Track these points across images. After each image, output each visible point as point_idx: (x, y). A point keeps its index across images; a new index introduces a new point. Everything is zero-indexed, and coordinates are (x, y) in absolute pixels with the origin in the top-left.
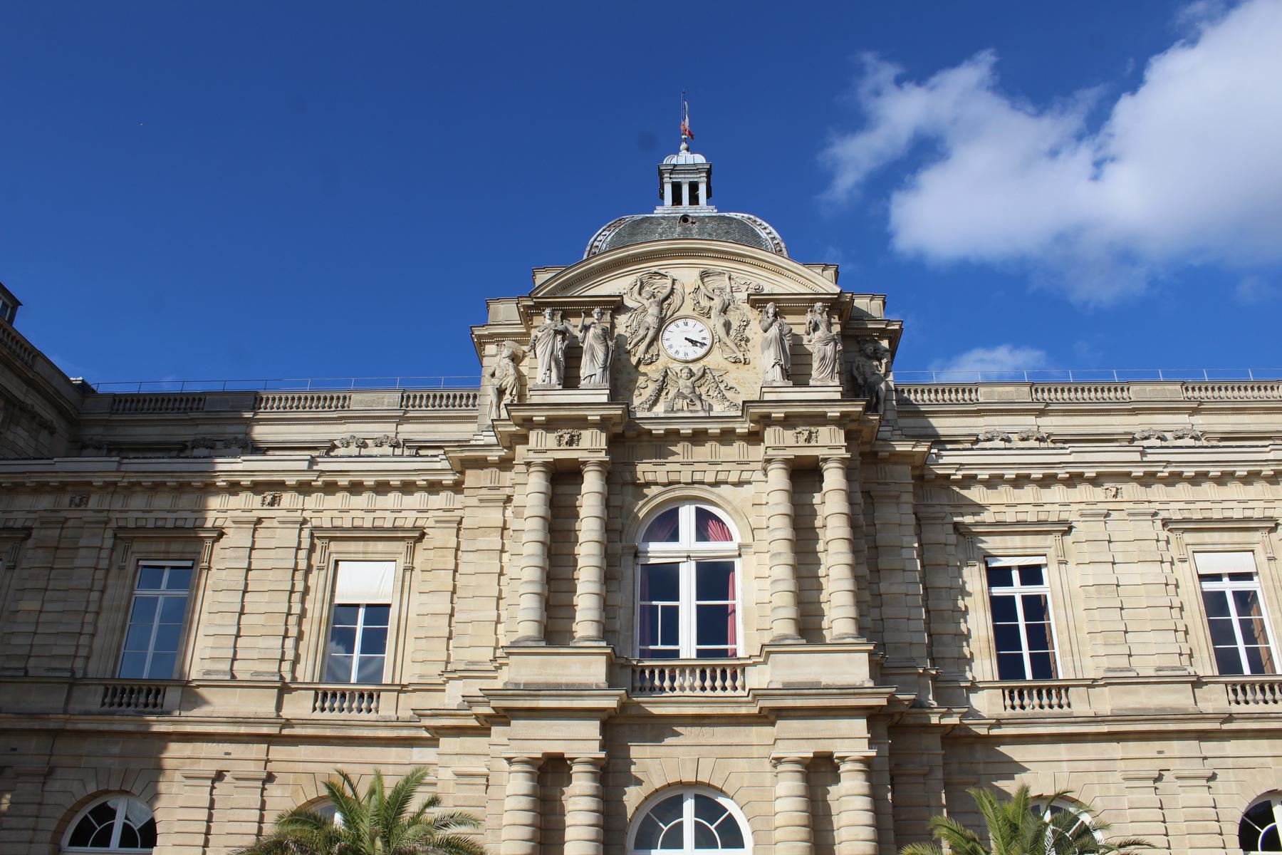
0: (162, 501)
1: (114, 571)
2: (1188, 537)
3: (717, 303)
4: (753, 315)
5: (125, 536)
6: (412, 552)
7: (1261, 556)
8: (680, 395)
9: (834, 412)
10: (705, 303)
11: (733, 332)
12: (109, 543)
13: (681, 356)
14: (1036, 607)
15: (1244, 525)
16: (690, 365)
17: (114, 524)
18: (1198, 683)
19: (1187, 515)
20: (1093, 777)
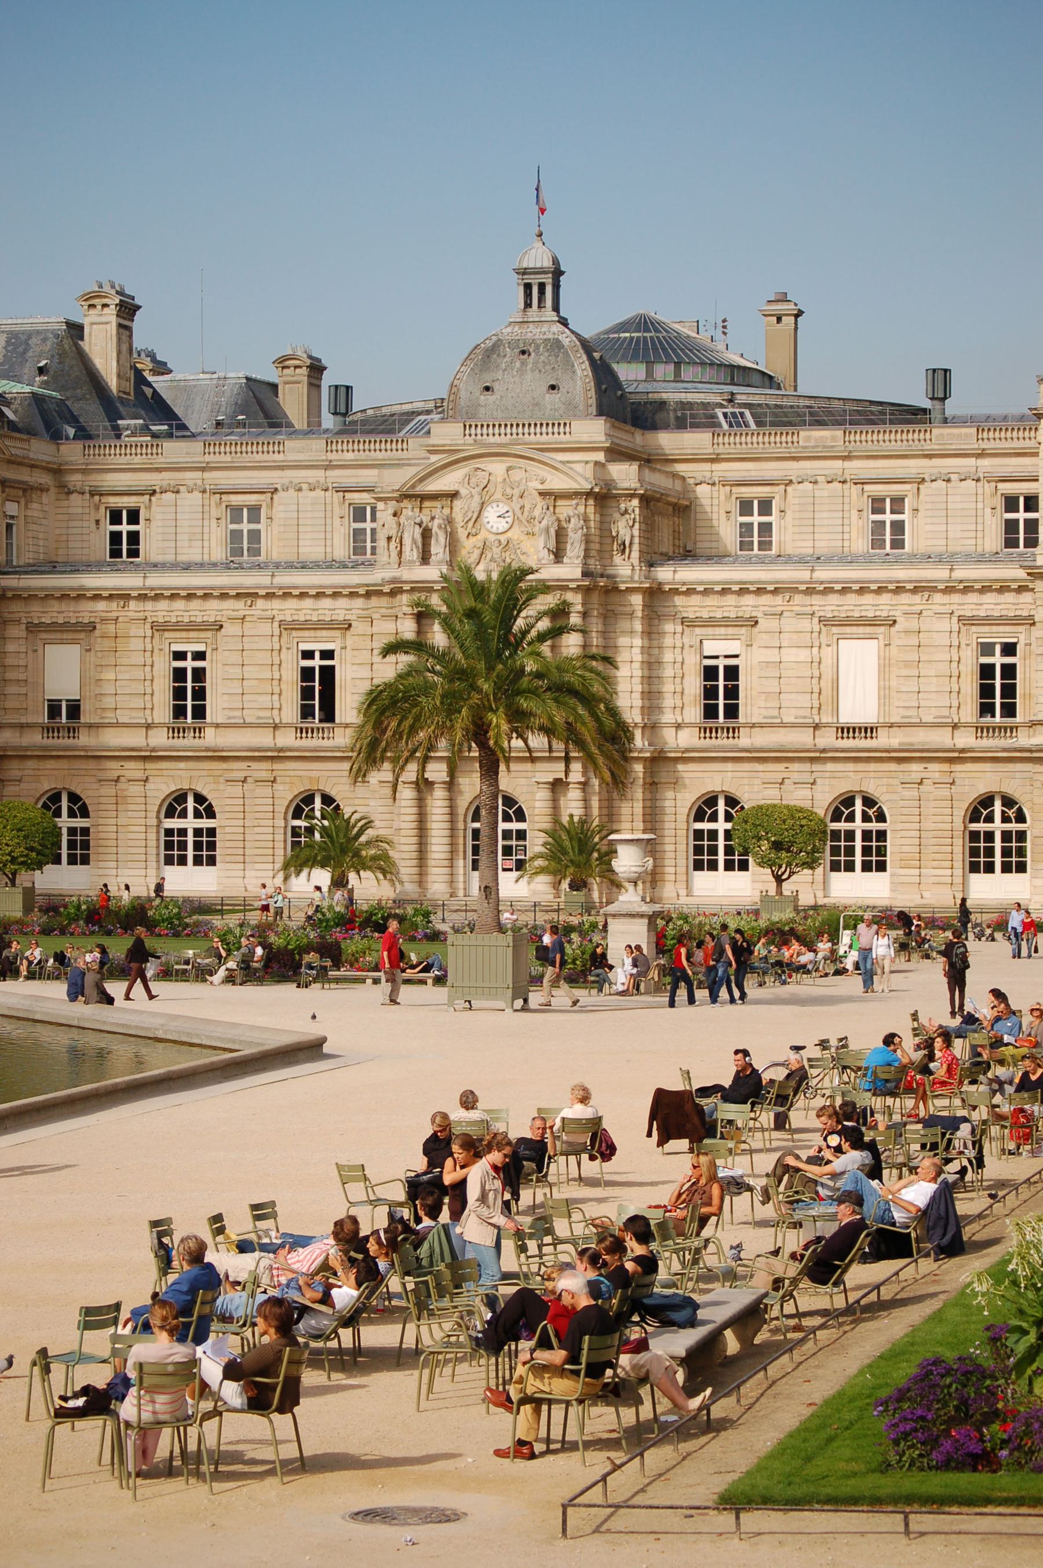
0: (179, 604)
1: (156, 651)
2: (835, 630)
3: (516, 492)
4: (539, 499)
5: (160, 628)
6: (344, 636)
7: (882, 643)
8: (492, 560)
9: (573, 585)
10: (509, 491)
11: (526, 513)
12: (149, 633)
13: (494, 530)
14: (732, 673)
15: (873, 622)
16: (500, 537)
17: (150, 620)
18: (816, 727)
19: (836, 614)
20: (746, 781)
